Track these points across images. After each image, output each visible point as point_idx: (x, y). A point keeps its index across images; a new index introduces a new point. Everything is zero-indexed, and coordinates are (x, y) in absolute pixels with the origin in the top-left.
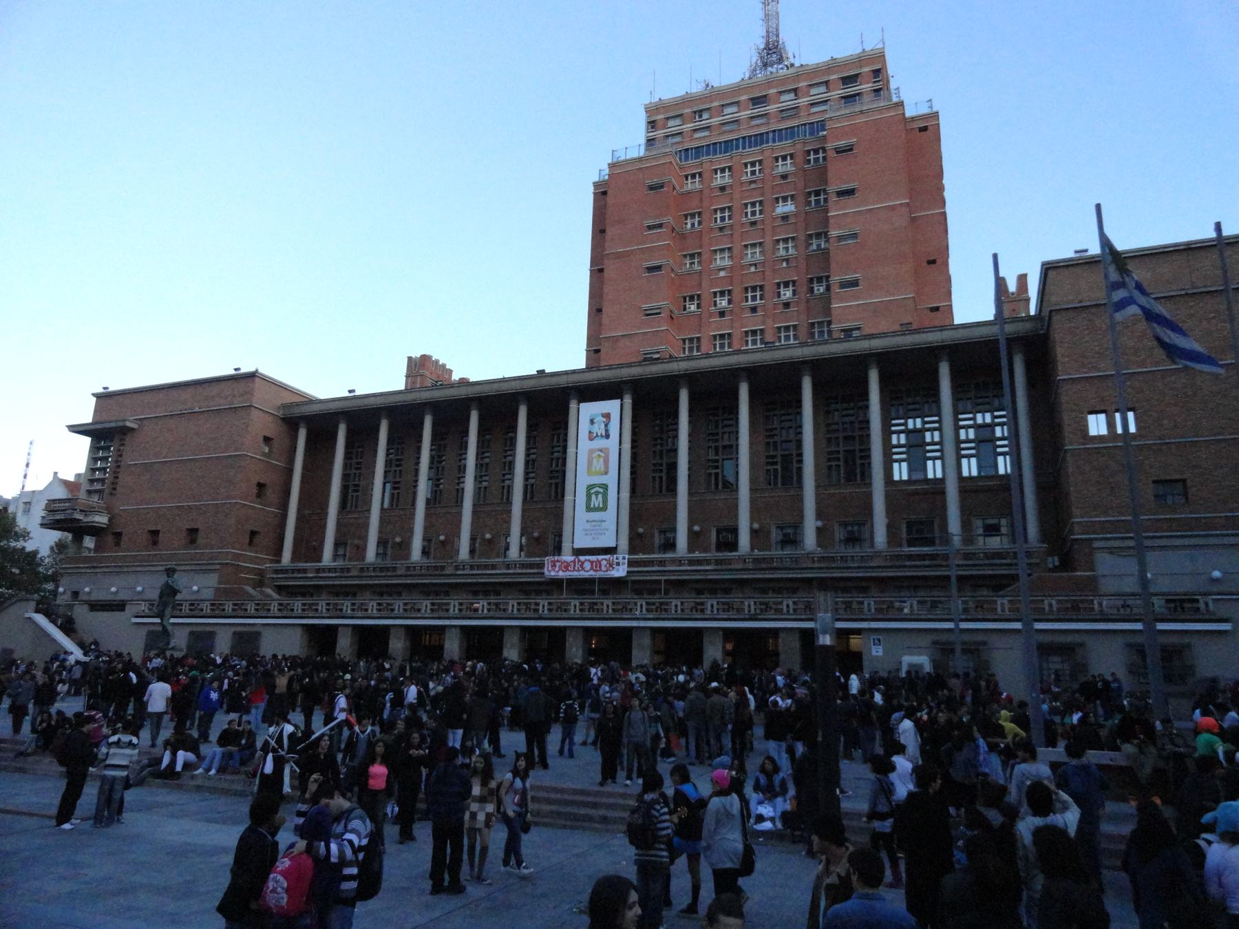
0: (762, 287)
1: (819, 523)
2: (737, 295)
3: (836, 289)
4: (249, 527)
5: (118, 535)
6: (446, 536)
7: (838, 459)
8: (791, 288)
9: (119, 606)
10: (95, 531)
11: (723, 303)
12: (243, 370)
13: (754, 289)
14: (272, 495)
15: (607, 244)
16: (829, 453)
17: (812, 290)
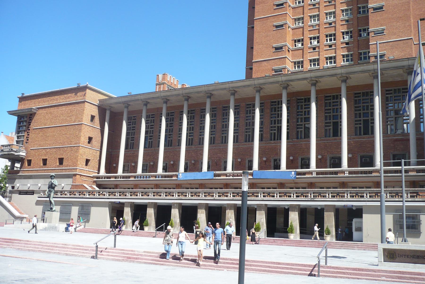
0: (335, 35)
1: (350, 156)
2: (323, 38)
3: (372, 34)
4: (85, 157)
5: (29, 162)
6: (174, 162)
7: (360, 124)
8: (350, 34)
9: (32, 193)
10: (20, 160)
11: (315, 43)
12: (81, 85)
13: (331, 35)
14: (96, 142)
15: (256, 14)
16: (356, 121)
17: (360, 35)
